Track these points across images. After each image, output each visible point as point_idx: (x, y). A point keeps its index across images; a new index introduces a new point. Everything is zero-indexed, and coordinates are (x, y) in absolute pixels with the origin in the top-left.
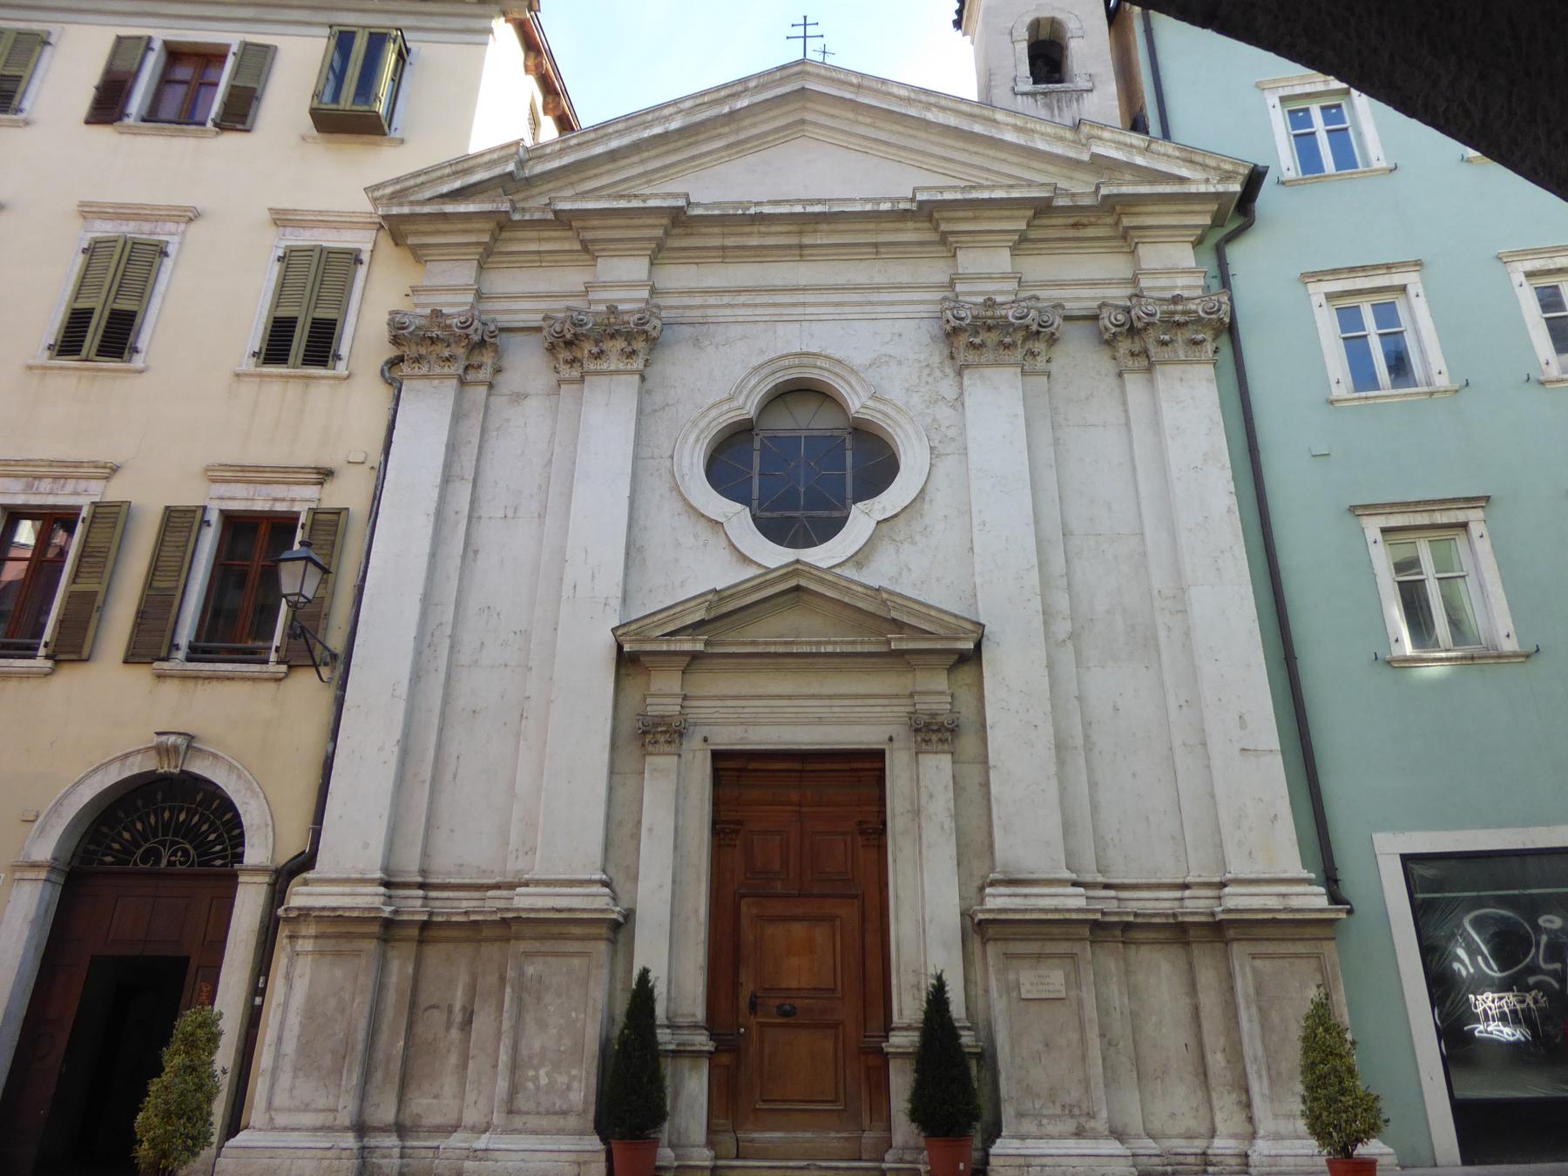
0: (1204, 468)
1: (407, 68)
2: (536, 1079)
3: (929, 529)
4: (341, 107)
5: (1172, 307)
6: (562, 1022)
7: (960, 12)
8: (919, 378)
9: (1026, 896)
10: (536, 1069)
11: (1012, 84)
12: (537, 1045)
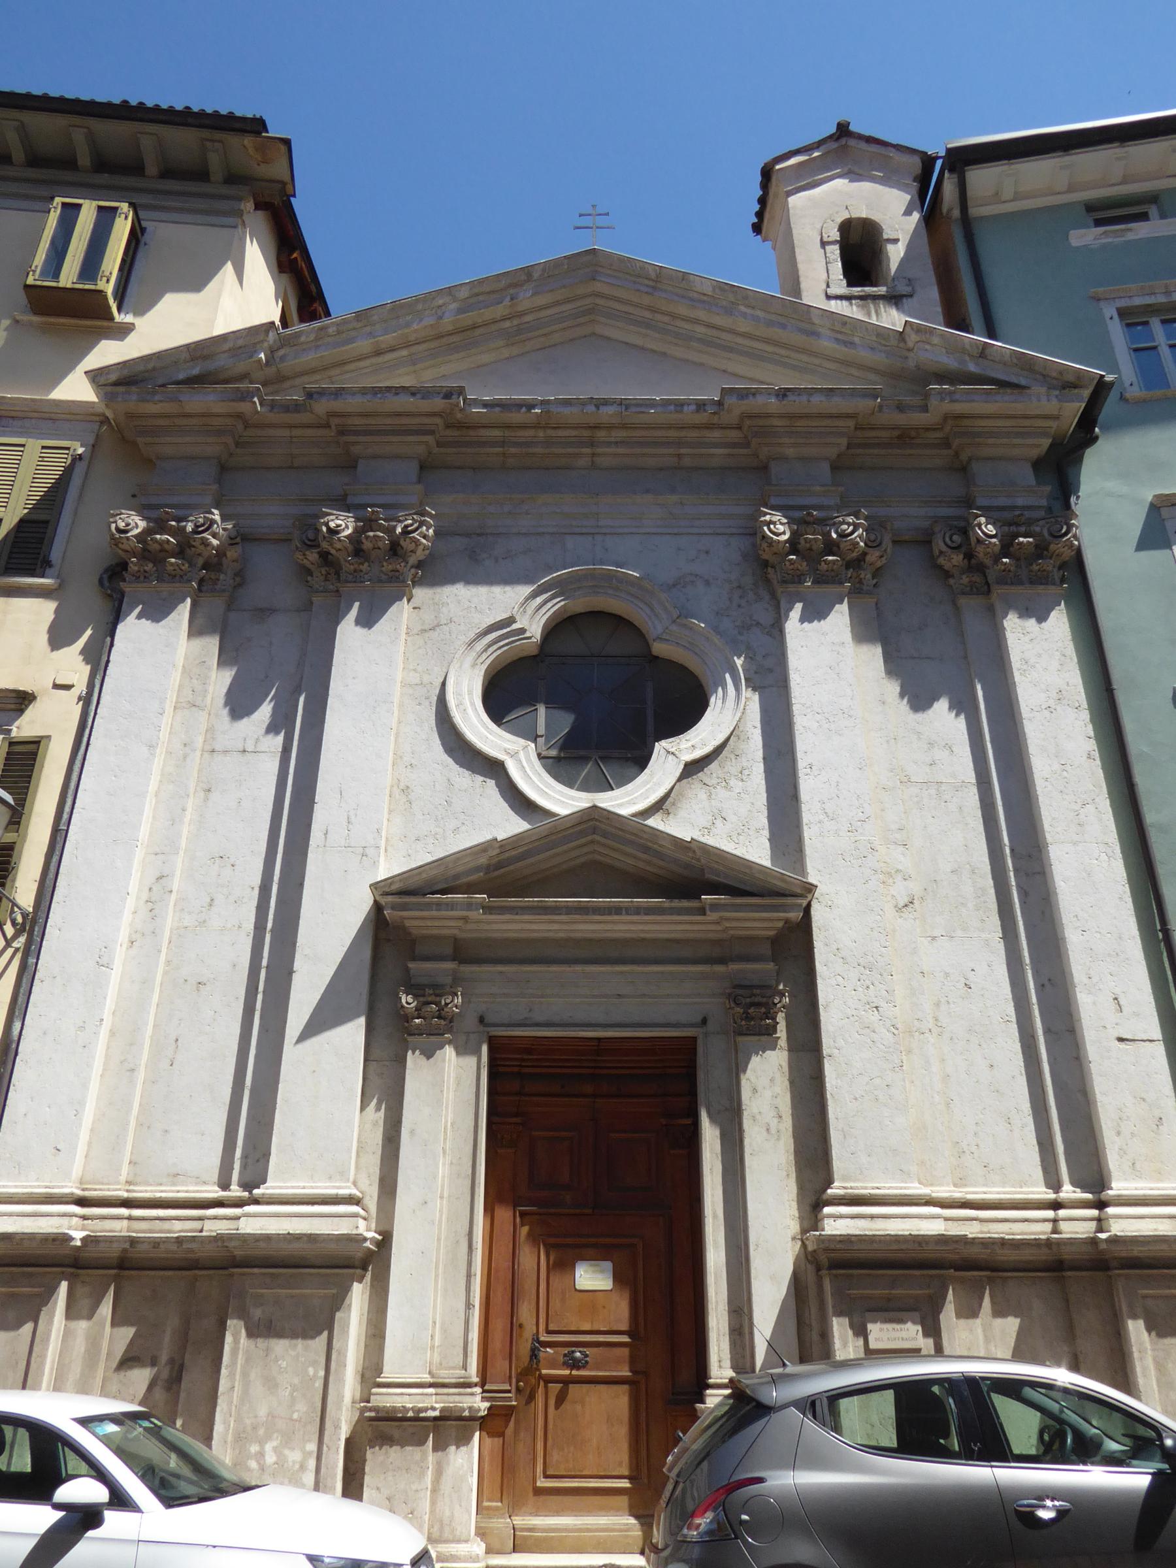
0: (1058, 708)
1: (141, 249)
2: (261, 1455)
3: (746, 772)
4: (61, 285)
5: (1013, 529)
6: (296, 1381)
7: (760, 215)
8: (730, 599)
9: (872, 1217)
10: (262, 1443)
11: (824, 286)
12: (262, 1412)
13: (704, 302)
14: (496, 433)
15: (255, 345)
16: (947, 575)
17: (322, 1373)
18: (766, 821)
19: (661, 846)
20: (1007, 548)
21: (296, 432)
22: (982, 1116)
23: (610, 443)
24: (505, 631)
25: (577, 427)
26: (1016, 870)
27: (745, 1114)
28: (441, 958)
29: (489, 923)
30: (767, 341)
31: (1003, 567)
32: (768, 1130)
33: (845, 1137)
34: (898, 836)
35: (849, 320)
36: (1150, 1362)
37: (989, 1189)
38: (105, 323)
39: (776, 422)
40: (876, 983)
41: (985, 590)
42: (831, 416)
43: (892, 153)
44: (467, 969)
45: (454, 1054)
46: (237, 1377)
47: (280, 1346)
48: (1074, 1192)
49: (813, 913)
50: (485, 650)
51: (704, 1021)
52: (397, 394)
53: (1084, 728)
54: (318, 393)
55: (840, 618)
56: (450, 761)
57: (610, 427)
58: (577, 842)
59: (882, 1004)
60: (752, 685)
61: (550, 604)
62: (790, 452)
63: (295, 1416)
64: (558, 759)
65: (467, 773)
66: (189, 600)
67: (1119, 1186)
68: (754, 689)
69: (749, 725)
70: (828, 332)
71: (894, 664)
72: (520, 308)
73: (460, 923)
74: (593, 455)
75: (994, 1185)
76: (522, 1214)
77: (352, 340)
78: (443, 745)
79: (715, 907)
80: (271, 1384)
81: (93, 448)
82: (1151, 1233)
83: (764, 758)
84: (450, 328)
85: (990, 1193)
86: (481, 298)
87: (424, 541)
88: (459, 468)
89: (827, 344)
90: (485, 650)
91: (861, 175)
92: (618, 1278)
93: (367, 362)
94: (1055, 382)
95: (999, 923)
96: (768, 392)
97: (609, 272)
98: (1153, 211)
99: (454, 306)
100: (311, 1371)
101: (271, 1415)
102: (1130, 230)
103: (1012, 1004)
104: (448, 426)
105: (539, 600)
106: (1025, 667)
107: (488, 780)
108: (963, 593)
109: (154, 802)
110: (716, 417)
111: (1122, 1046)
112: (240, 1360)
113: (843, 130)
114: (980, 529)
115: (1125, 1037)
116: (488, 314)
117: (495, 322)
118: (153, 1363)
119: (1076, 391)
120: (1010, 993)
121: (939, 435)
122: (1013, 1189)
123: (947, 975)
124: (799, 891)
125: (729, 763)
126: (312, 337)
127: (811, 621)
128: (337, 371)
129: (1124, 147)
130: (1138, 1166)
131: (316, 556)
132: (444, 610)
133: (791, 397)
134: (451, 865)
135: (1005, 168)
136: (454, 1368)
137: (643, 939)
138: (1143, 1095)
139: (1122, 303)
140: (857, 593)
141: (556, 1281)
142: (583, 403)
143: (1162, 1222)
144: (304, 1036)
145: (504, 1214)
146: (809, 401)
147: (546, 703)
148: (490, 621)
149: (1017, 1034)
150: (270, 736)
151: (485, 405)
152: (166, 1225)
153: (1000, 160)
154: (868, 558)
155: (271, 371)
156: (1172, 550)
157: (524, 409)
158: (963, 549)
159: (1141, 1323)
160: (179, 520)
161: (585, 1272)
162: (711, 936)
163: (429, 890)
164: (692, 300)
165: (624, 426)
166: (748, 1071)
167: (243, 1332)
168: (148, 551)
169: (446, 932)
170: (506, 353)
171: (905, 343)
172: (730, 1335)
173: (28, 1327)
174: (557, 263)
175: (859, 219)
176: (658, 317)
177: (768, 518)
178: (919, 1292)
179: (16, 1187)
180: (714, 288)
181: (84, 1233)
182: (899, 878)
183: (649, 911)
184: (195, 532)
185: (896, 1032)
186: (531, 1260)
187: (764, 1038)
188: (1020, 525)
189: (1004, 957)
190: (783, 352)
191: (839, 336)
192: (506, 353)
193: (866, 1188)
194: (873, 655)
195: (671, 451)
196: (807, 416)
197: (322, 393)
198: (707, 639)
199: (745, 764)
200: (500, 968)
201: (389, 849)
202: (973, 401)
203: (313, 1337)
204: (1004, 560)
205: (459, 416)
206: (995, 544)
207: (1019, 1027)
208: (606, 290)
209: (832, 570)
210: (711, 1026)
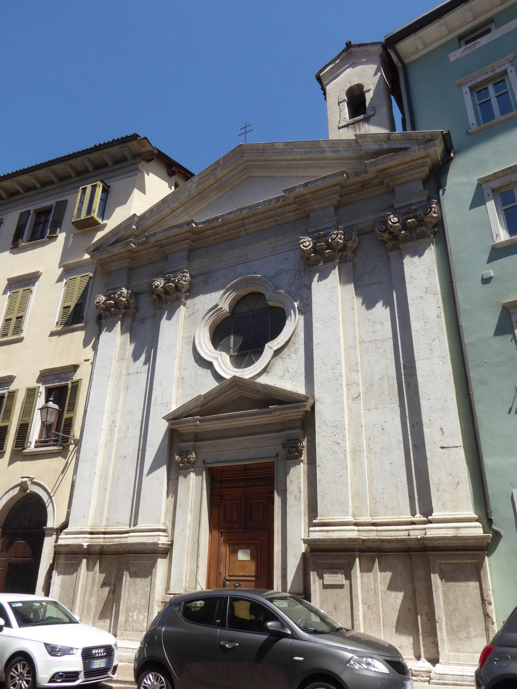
0: (425, 296)
2: (133, 616)
3: (297, 350)
4: (81, 219)
6: (142, 592)
8: (295, 277)
9: (328, 531)
10: (133, 613)
12: (133, 602)
13: (281, 152)
14: (210, 231)
15: (131, 224)
16: (385, 242)
17: (149, 590)
18: (304, 370)
19: (258, 388)
20: (405, 226)
21: (149, 250)
22: (385, 486)
23: (250, 223)
24: (215, 310)
25: (238, 221)
26: (405, 375)
27: (288, 491)
28: (189, 441)
29: (204, 426)
30: (309, 159)
31: (403, 235)
32: (296, 497)
33: (323, 499)
34: (355, 367)
35: (335, 142)
36: (440, 592)
37: (386, 517)
38: (98, 226)
39: (308, 196)
40: (339, 433)
41: (396, 248)
42: (329, 187)
43: (369, 48)
44: (198, 444)
45: (195, 475)
46: (126, 591)
47: (138, 580)
48: (420, 517)
49: (316, 406)
50: (209, 319)
51: (277, 455)
52: (173, 229)
53: (437, 303)
54: (149, 236)
55: (335, 275)
56: (196, 365)
57: (249, 217)
58: (231, 390)
59: (340, 442)
60: (301, 312)
61: (231, 295)
62: (317, 206)
63: (142, 604)
64: (237, 356)
65: (202, 368)
66: (119, 322)
67: (436, 515)
68: (302, 315)
69: (299, 329)
70: (329, 149)
71: (359, 291)
72: (219, 177)
73: (194, 427)
74: (245, 229)
75: (389, 515)
76: (221, 533)
77: (162, 210)
78: (195, 359)
79: (275, 410)
80: (136, 593)
81: (95, 273)
82: (444, 536)
83: (305, 343)
84: (196, 194)
85: (386, 519)
86: (203, 179)
87: (184, 283)
88: (202, 248)
89: (329, 154)
90: (209, 319)
91: (357, 63)
92: (252, 556)
93: (171, 216)
94: (422, 141)
95: (398, 399)
96: (300, 186)
97: (247, 152)
98: (493, 26)
99: (194, 185)
100: (146, 589)
101: (136, 603)
102: (477, 43)
103: (402, 435)
104: (194, 234)
105: (227, 295)
106: (411, 280)
107: (208, 370)
108: (391, 250)
109: (111, 396)
110: (285, 202)
111: (443, 450)
112: (127, 585)
113: (349, 45)
114: (391, 221)
115: (444, 446)
116: (208, 183)
117: (211, 185)
118: (110, 586)
119: (432, 142)
120: (401, 430)
121: (378, 180)
122: (397, 517)
123: (374, 425)
124: (304, 399)
125: (291, 348)
126: (149, 214)
127: (321, 281)
128: (161, 223)
130: (445, 504)
131: (155, 296)
132: (196, 306)
133: (309, 186)
134: (187, 407)
135: (414, 36)
136: (192, 588)
137: (257, 425)
138: (451, 472)
139: (471, 84)
140: (343, 261)
141: (232, 558)
142: (235, 212)
143: (450, 530)
144: (148, 474)
145: (216, 533)
146: (316, 185)
147: (234, 334)
148: (210, 307)
149: (403, 448)
150: (145, 365)
151: (203, 223)
152: (113, 540)
154: (348, 245)
155: (140, 230)
156: (486, 205)
157: (216, 221)
158: (387, 231)
159: (437, 576)
160: (114, 295)
161: (241, 554)
162: (280, 421)
163: (182, 417)
164: (277, 153)
165: (254, 215)
166: (290, 474)
167: (128, 576)
168: (107, 308)
169: (190, 431)
170: (218, 195)
171: (359, 144)
172: (282, 578)
173: (75, 573)
174: (227, 156)
175: (355, 85)
176: (269, 163)
177: (302, 241)
178: (344, 561)
179: (74, 529)
180: (283, 145)
181: (87, 544)
182: (355, 386)
183: (254, 414)
184: (118, 298)
185: (345, 453)
186: (225, 550)
187: (296, 460)
188: (410, 213)
189: (400, 414)
190: (316, 162)
191: (333, 149)
192: (218, 195)
193: (329, 519)
194: (351, 288)
195: (273, 220)
196: (320, 190)
197: (150, 236)
198: (285, 296)
199: (297, 347)
200: (208, 442)
201: (177, 402)
202: (385, 162)
203: (147, 577)
204: (402, 232)
205: (196, 230)
206: (398, 226)
207: (404, 445)
208: (249, 159)
209: (331, 256)
210: (280, 457)
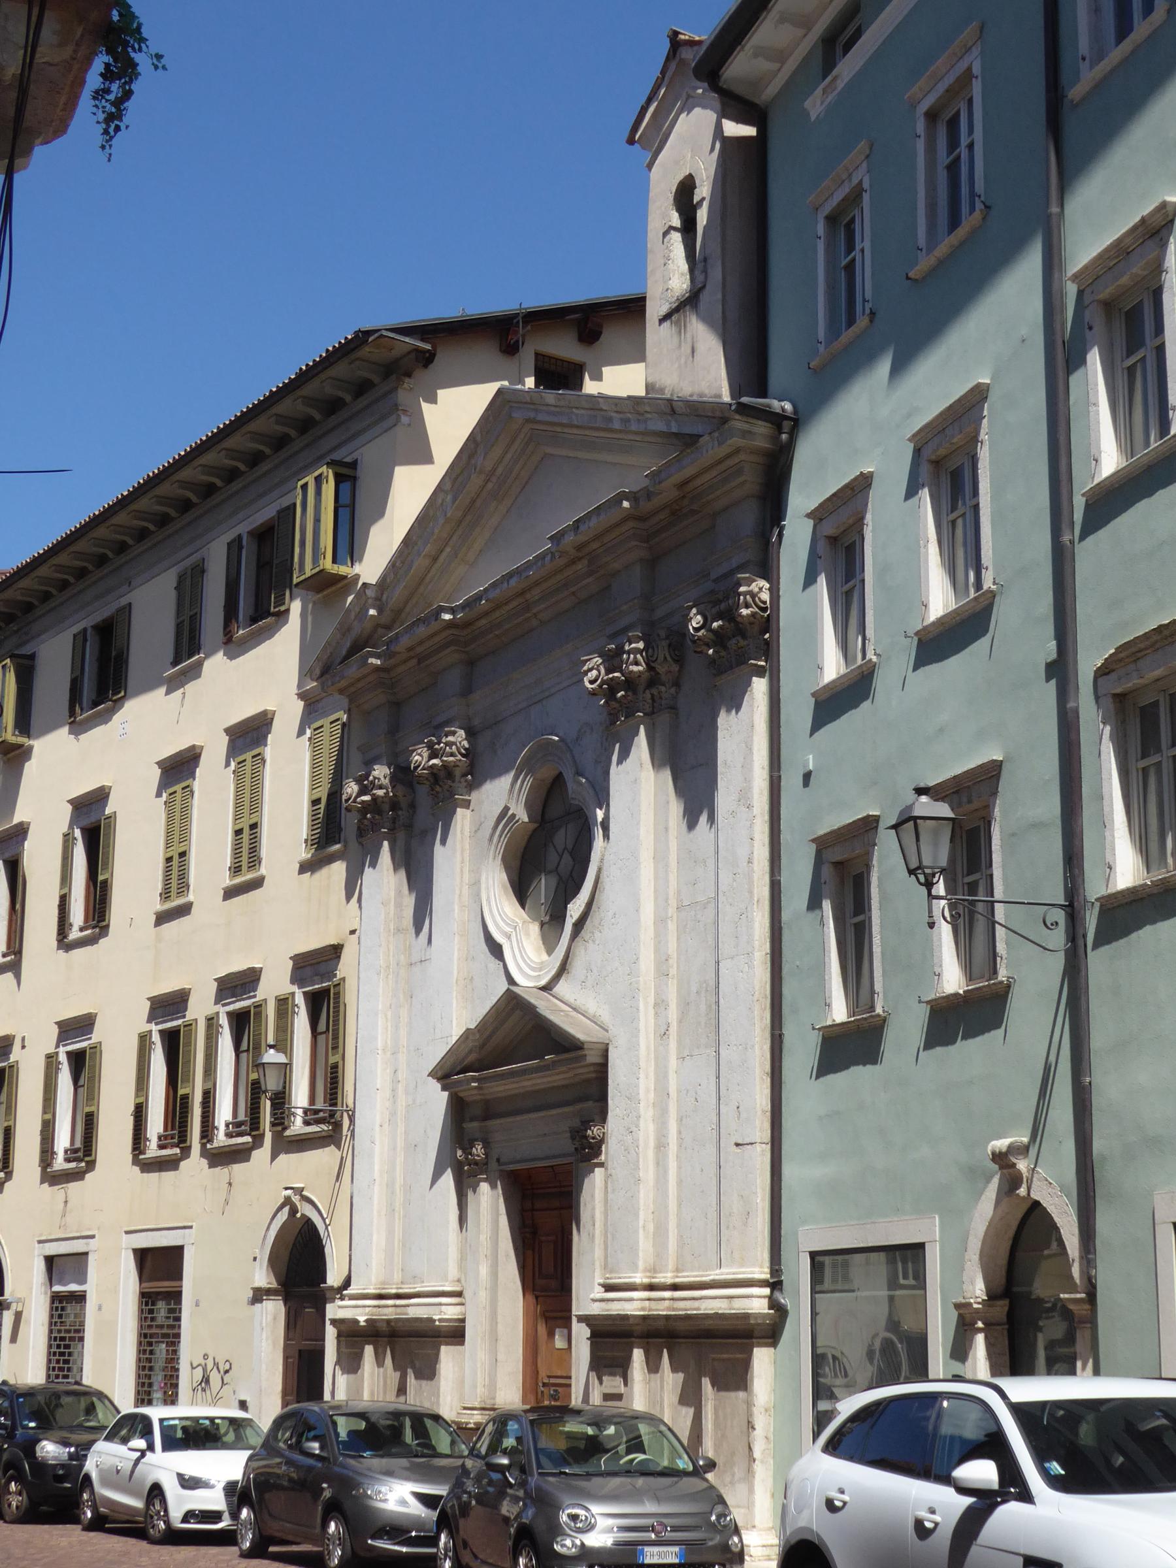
38: (346, 582)
76: (537, 1297)
81: (349, 712)
84: (460, 514)
99: (449, 498)
129: (771, 10)
133: (582, 528)
137: (553, 1088)
139: (827, 209)
153: (731, 53)
181: (366, 1318)
186: (542, 1329)
